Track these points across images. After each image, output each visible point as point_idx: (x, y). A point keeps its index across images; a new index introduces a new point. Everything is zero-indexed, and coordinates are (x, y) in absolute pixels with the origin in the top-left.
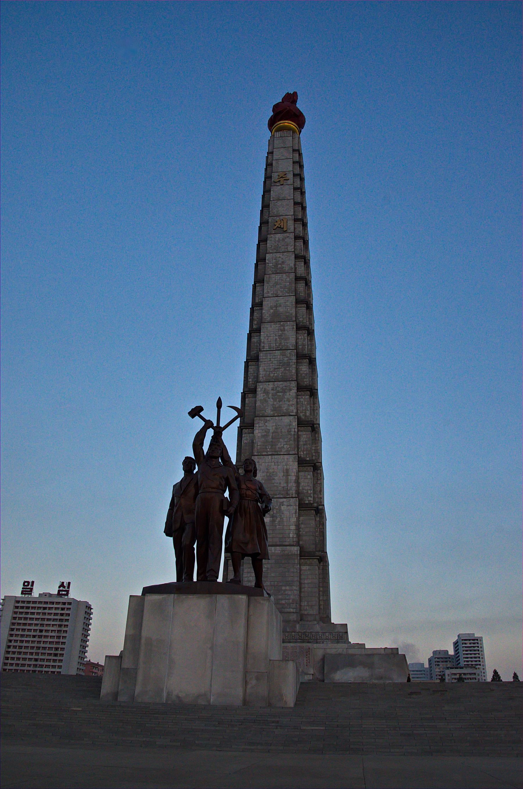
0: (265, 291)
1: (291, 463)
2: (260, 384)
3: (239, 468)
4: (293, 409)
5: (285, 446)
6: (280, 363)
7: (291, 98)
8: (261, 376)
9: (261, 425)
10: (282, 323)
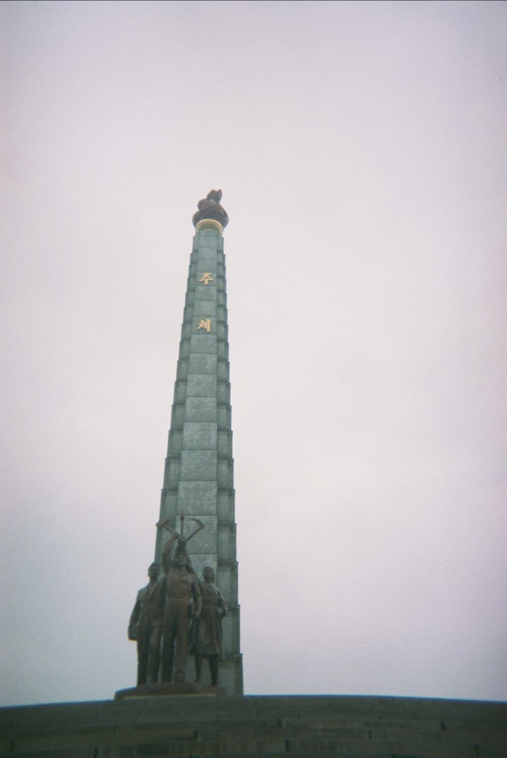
0: (188, 390)
2: (181, 482)
4: (213, 508)
7: (215, 196)
8: (183, 474)
10: (204, 423)
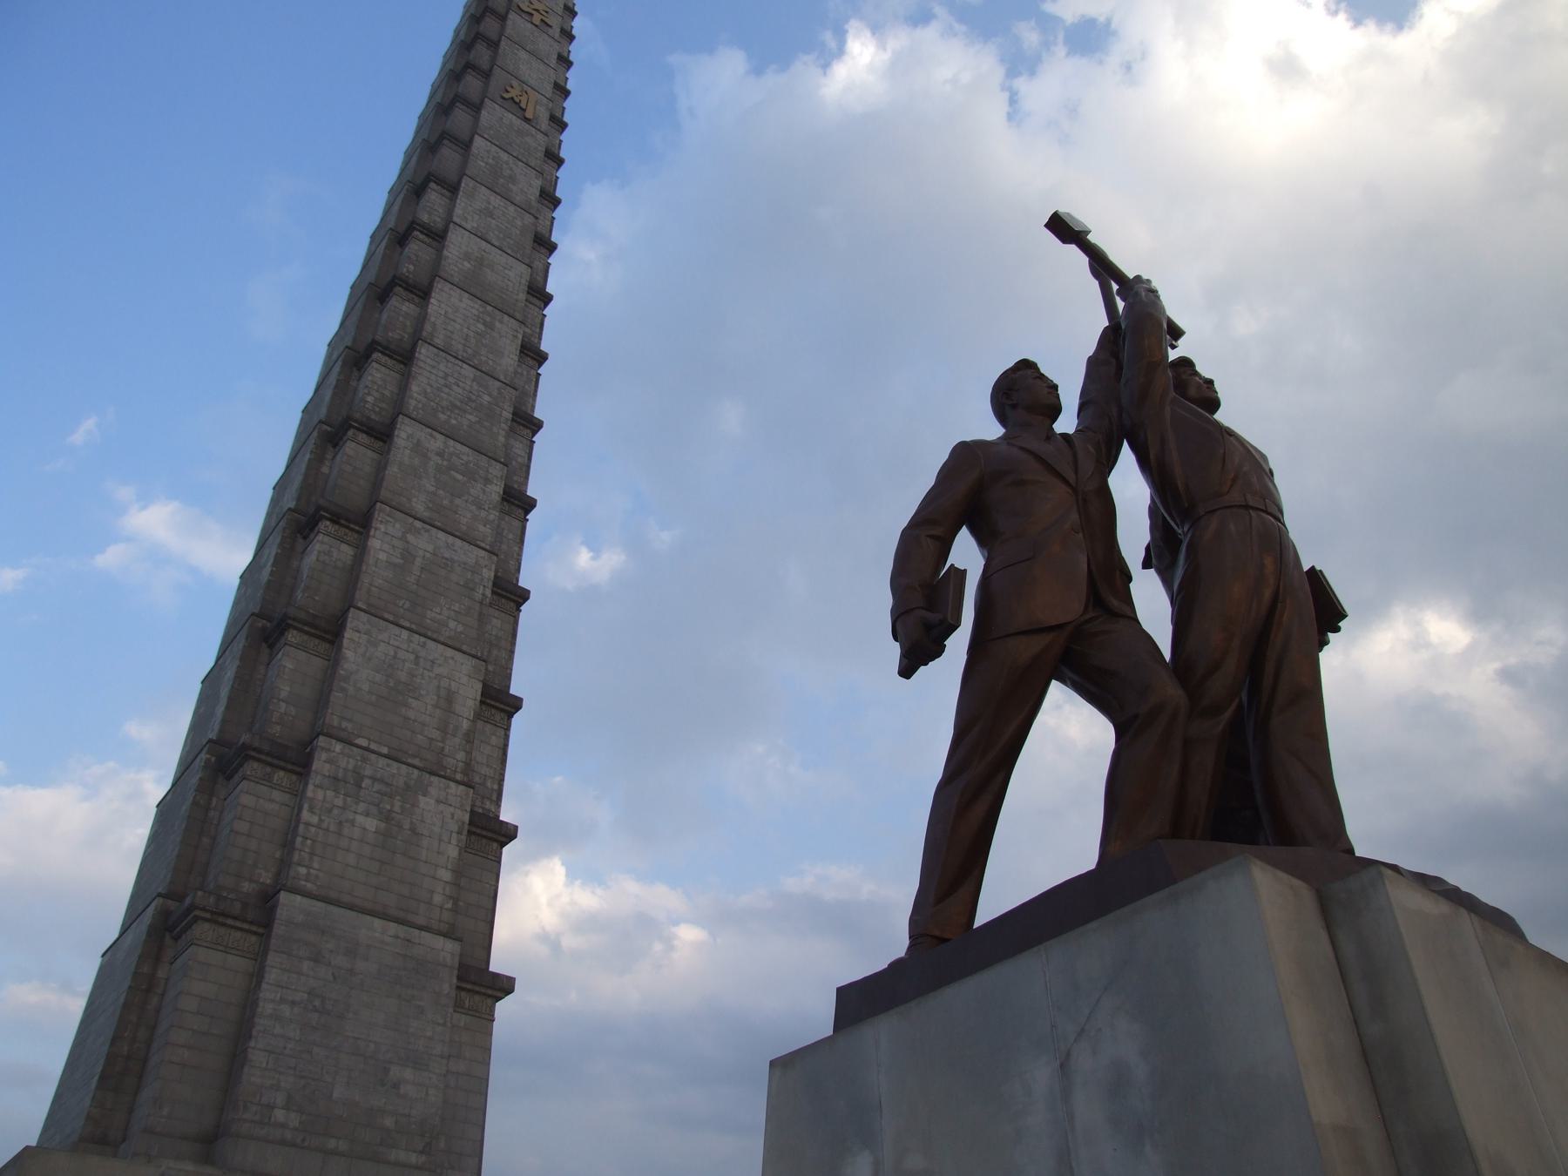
0: (458, 211)
1: (465, 680)
2: (407, 420)
3: (290, 626)
5: (452, 624)
6: (470, 399)
9: (390, 530)
